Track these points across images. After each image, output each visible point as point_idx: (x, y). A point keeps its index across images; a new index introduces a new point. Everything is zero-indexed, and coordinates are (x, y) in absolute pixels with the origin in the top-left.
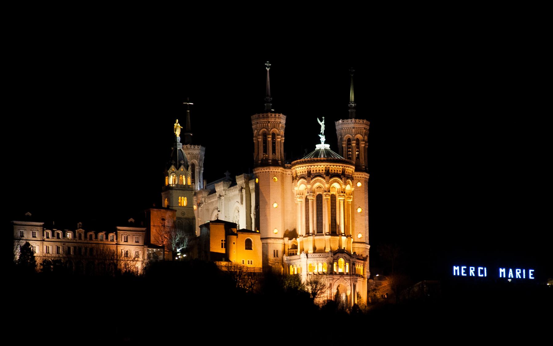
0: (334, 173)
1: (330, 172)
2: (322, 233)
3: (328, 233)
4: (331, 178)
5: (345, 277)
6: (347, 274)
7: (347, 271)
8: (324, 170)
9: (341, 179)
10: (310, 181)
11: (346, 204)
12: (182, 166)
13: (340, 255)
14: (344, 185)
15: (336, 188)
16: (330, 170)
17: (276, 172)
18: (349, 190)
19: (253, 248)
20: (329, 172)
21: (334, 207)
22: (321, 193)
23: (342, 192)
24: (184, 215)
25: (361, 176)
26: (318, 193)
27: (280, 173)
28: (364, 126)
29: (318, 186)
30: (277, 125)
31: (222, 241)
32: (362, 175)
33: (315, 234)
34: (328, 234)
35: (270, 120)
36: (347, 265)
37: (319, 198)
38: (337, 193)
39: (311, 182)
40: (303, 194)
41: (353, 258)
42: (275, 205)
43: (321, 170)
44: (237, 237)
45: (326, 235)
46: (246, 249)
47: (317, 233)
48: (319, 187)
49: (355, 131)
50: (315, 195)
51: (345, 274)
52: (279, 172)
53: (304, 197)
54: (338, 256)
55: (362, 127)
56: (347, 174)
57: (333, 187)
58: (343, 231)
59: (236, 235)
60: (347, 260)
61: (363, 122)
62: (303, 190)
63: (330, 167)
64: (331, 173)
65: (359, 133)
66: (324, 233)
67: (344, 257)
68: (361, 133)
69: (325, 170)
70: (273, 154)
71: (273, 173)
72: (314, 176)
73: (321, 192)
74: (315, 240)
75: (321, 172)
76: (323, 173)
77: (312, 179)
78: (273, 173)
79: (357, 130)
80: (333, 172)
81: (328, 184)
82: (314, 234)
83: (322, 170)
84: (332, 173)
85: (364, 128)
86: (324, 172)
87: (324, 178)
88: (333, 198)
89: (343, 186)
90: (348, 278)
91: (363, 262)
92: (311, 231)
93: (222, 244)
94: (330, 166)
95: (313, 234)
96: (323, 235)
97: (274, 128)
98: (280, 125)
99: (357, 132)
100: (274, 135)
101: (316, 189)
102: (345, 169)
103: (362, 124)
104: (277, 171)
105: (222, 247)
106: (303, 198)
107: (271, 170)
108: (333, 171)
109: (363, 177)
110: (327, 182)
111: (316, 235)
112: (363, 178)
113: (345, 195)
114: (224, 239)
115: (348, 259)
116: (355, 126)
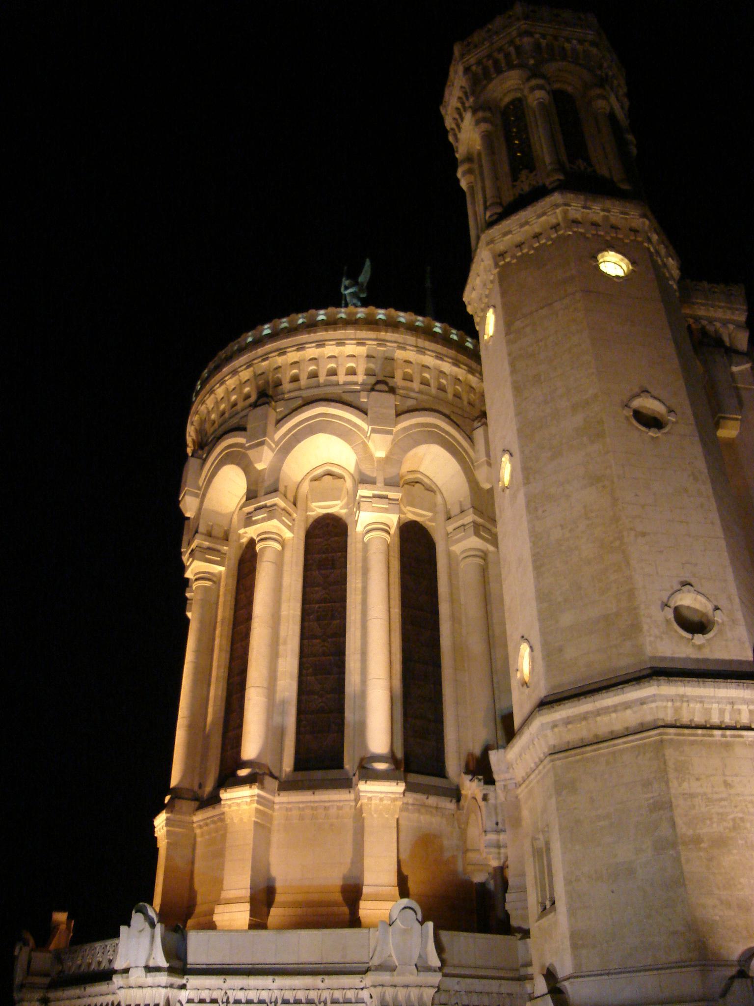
2: (341, 766)
8: (361, 370)
10: (270, 427)
15: (439, 497)
22: (336, 507)
26: (319, 509)
29: (319, 471)
34: (381, 766)
38: (441, 517)
39: (277, 436)
40: (226, 538)
43: (342, 372)
45: (367, 773)
47: (301, 764)
48: (329, 474)
50: (295, 515)
53: (231, 551)
57: (417, 482)
62: (234, 513)
63: (400, 354)
66: (350, 764)
69: (369, 373)
72: (299, 402)
73: (338, 499)
75: (342, 378)
76: (356, 383)
77: (279, 422)
81: (389, 432)
83: (352, 372)
86: (360, 378)
87: (363, 411)
92: (251, 748)
96: (346, 784)
101: (305, 487)
106: (223, 559)
110: (380, 424)
111: (287, 786)
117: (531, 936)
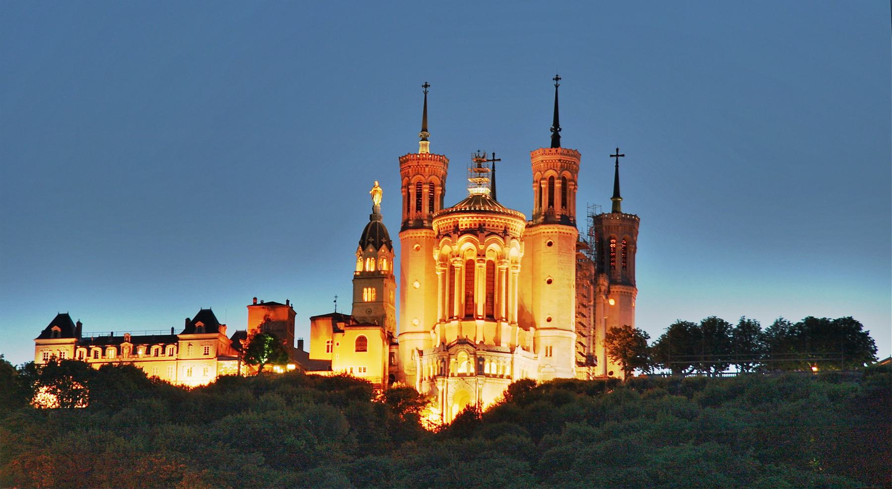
0: (466, 228)
1: (460, 227)
3: (456, 316)
4: (459, 236)
5: (467, 380)
6: (471, 375)
7: (473, 370)
8: (452, 226)
9: (477, 236)
11: (497, 272)
12: (370, 246)
13: (460, 347)
14: (480, 244)
16: (460, 225)
17: (419, 237)
18: (500, 252)
19: (367, 350)
20: (459, 228)
21: (472, 278)
23: (479, 255)
24: (370, 314)
25: (552, 230)
27: (424, 238)
28: (558, 157)
30: (421, 170)
31: (328, 342)
32: (554, 229)
33: (446, 321)
35: (410, 164)
36: (472, 360)
37: (452, 269)
41: (479, 350)
42: (417, 285)
44: (343, 335)
46: (357, 351)
49: (544, 165)
50: (447, 263)
51: (468, 375)
52: (423, 237)
54: (458, 350)
55: (555, 159)
56: (491, 227)
57: (470, 249)
58: (480, 311)
59: (343, 331)
60: (471, 354)
61: (557, 151)
64: (461, 229)
65: (551, 169)
67: (467, 350)
68: (554, 167)
69: (454, 226)
70: (416, 212)
71: (413, 238)
74: (446, 330)
78: (413, 238)
79: (547, 165)
80: (464, 227)
81: (455, 245)
82: (445, 321)
84: (463, 229)
85: (560, 160)
88: (470, 265)
89: (481, 247)
90: (473, 380)
91: (510, 355)
93: (328, 346)
94: (459, 218)
95: (443, 320)
97: (418, 174)
98: (427, 169)
99: (547, 167)
100: (419, 185)
102: (484, 221)
103: (555, 154)
104: (419, 235)
105: (328, 351)
107: (411, 235)
108: (464, 225)
109: (556, 232)
112: (554, 234)
113: (484, 259)
114: (330, 340)
115: (473, 353)
116: (544, 159)
117: (368, 349)
